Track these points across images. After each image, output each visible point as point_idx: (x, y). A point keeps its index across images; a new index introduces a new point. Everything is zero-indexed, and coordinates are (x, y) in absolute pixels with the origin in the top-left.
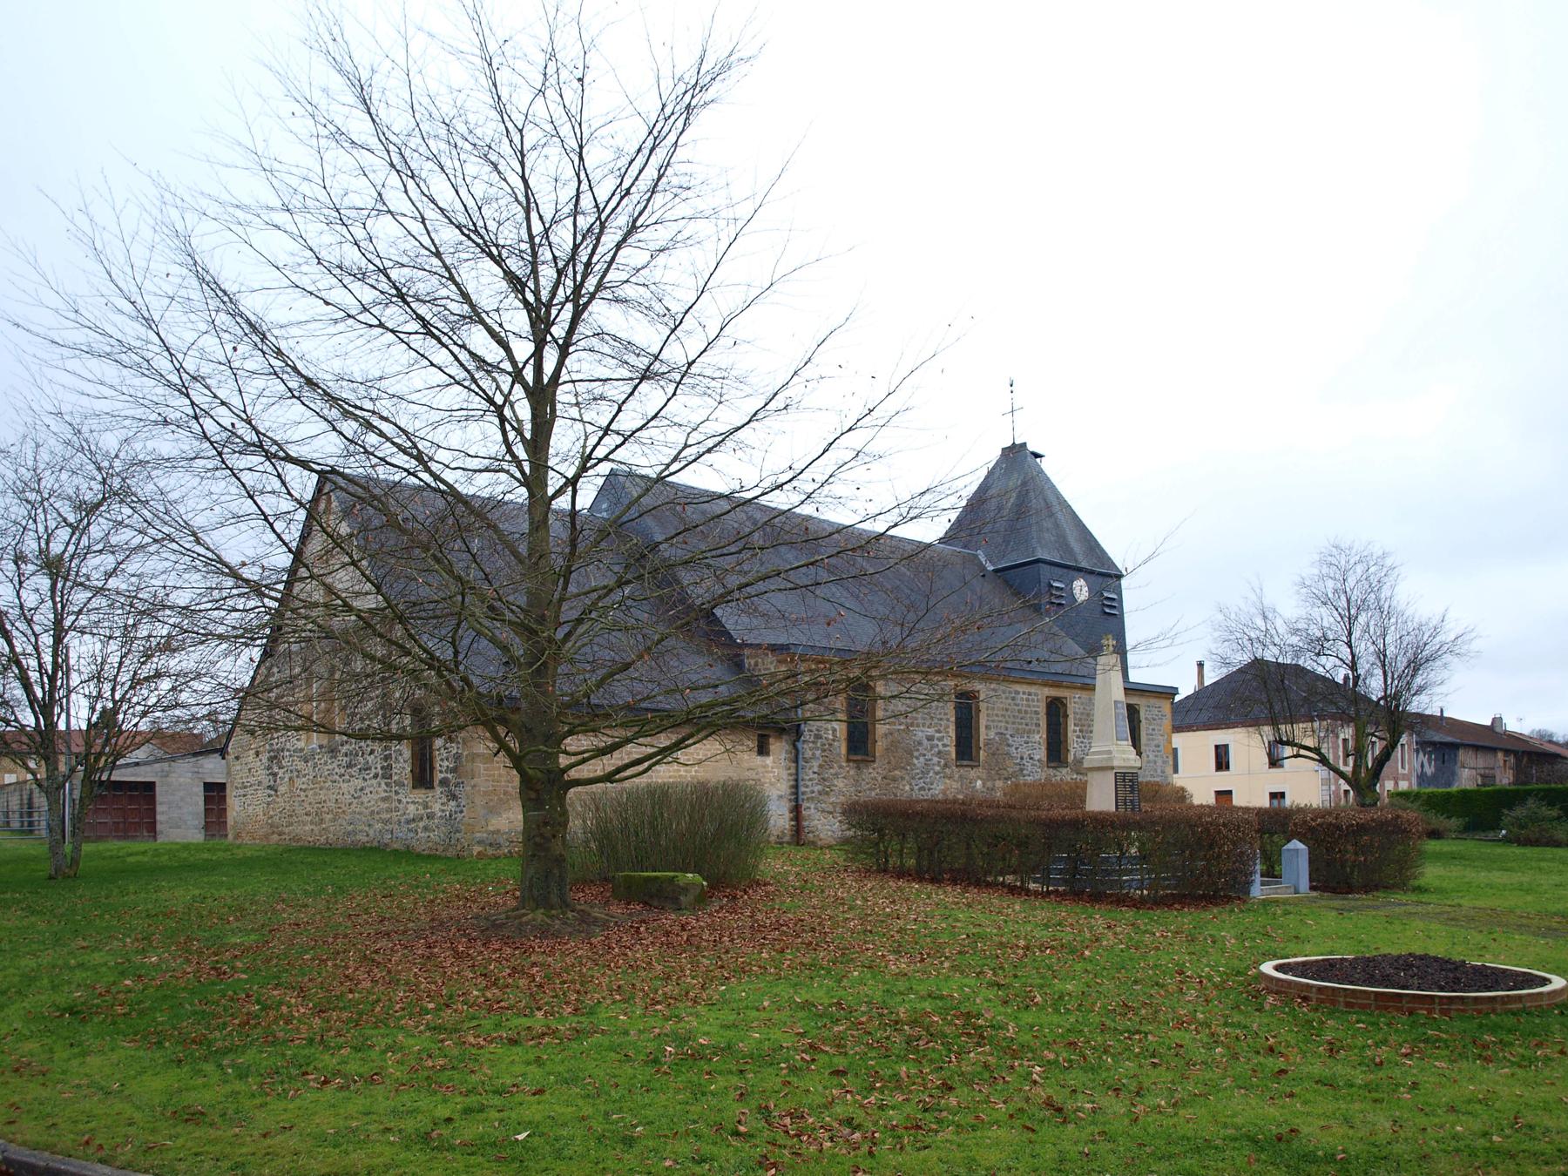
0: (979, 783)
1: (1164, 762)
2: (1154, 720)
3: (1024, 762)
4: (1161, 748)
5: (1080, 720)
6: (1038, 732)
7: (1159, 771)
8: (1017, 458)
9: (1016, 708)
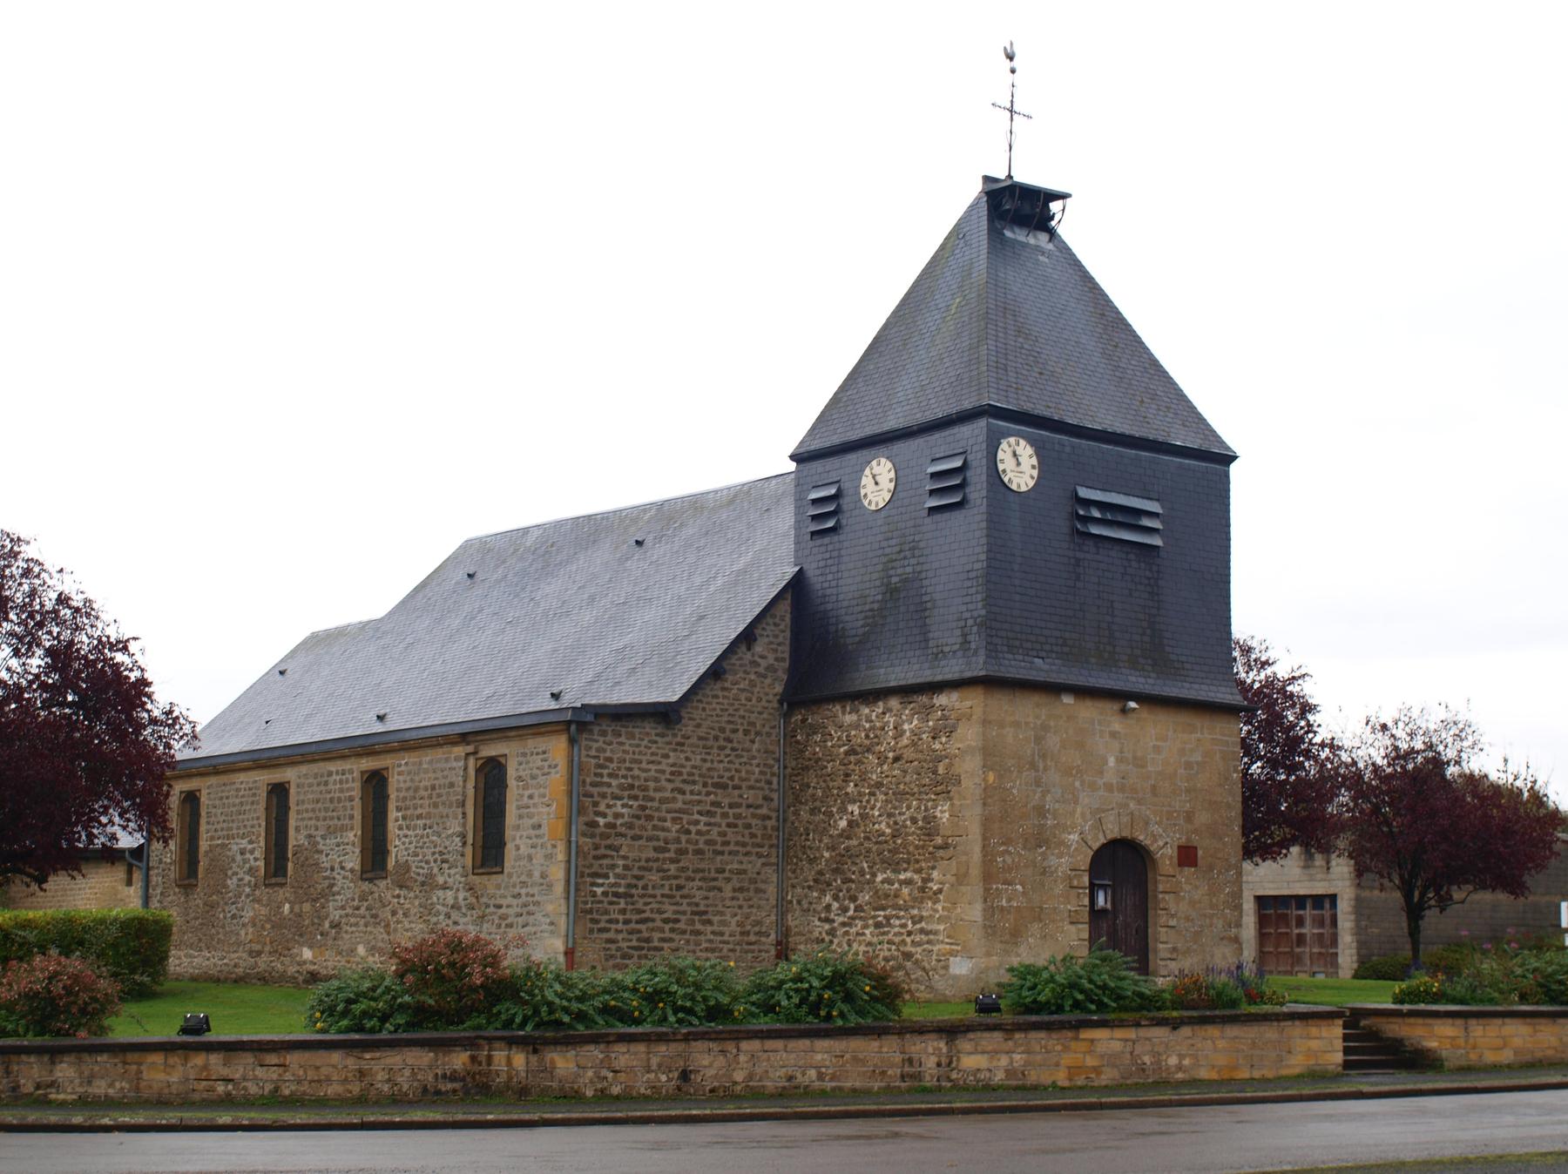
0: (287, 906)
1: (549, 857)
2: (533, 777)
3: (335, 874)
4: (544, 830)
5: (405, 799)
6: (352, 829)
7: (537, 874)
8: (987, 179)
9: (329, 796)
